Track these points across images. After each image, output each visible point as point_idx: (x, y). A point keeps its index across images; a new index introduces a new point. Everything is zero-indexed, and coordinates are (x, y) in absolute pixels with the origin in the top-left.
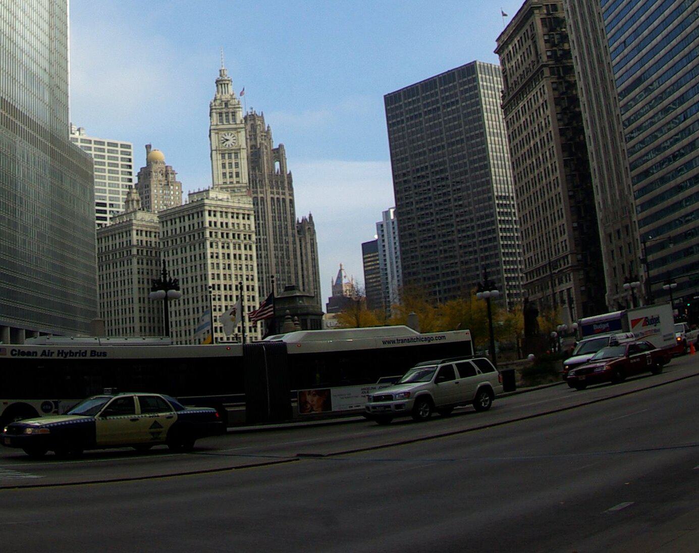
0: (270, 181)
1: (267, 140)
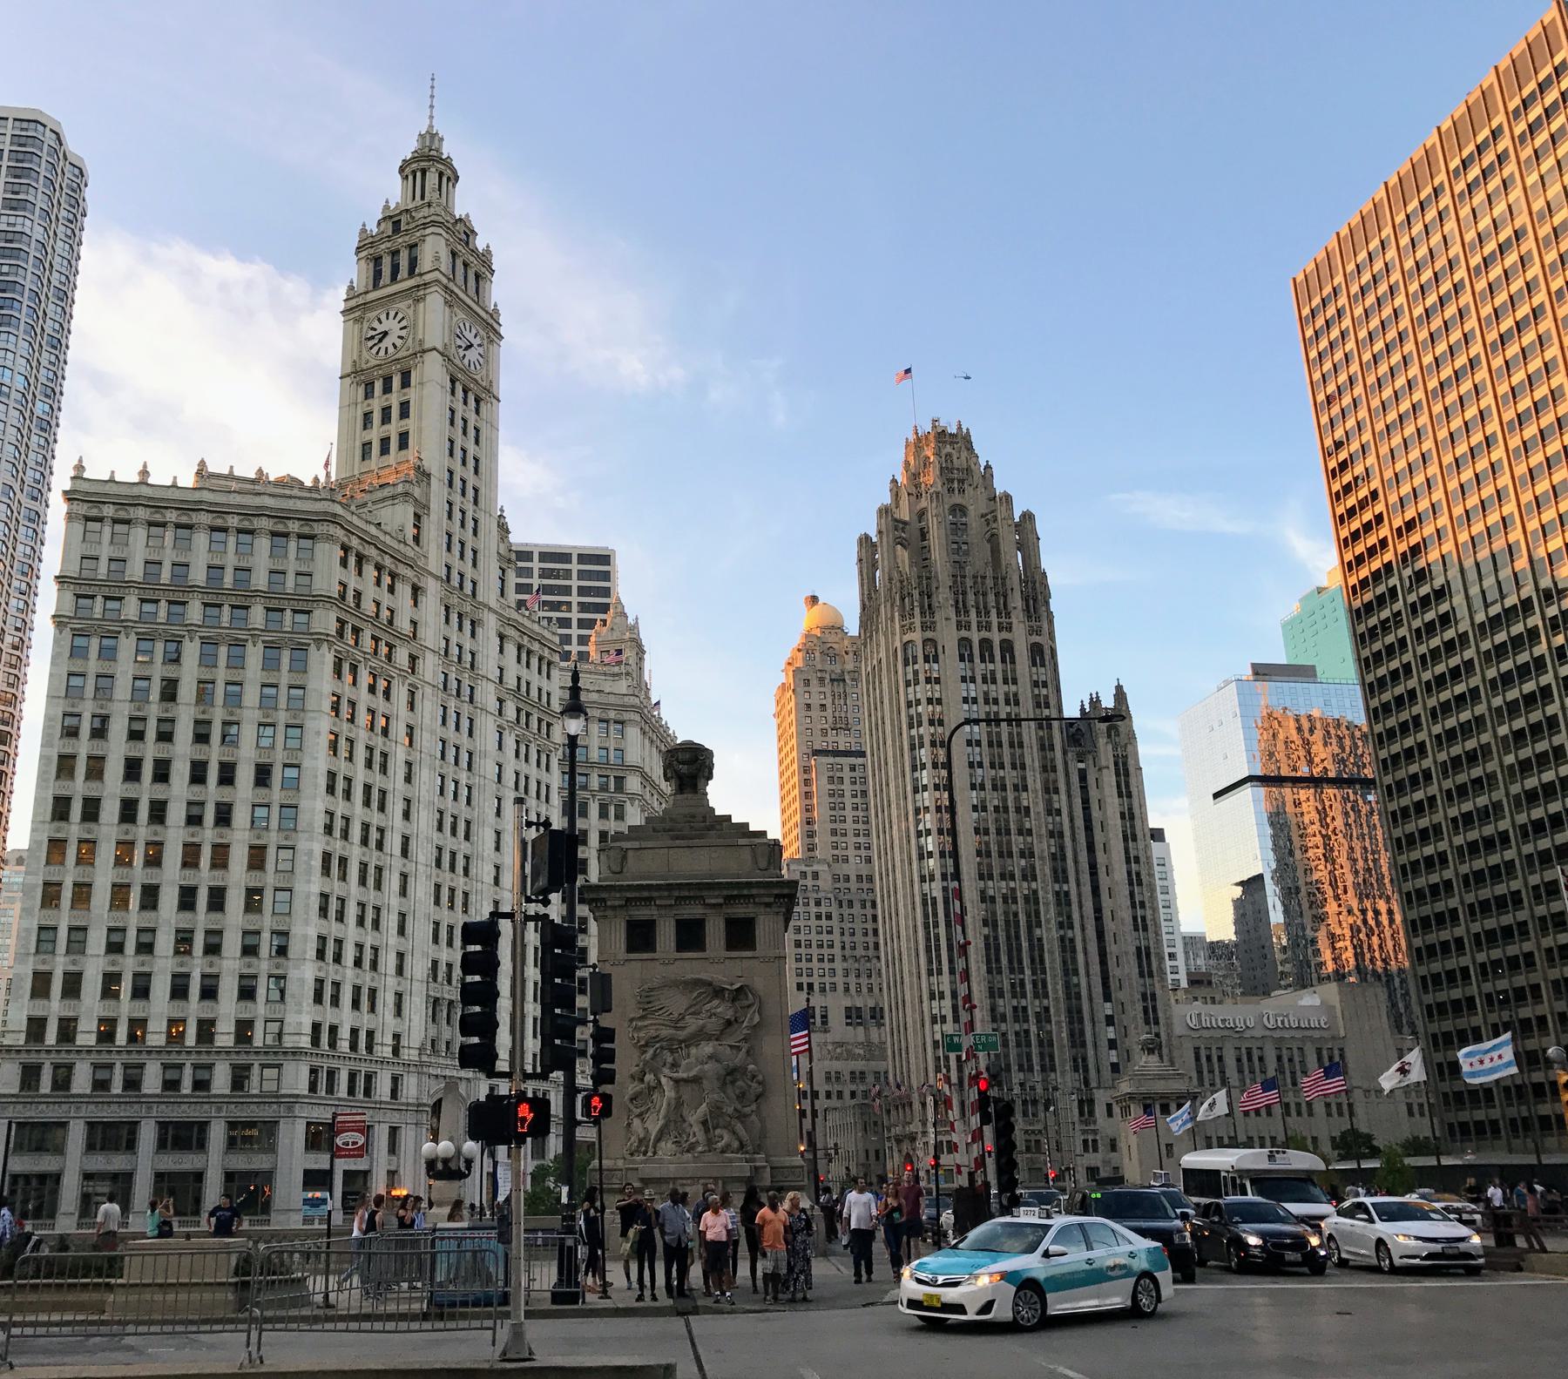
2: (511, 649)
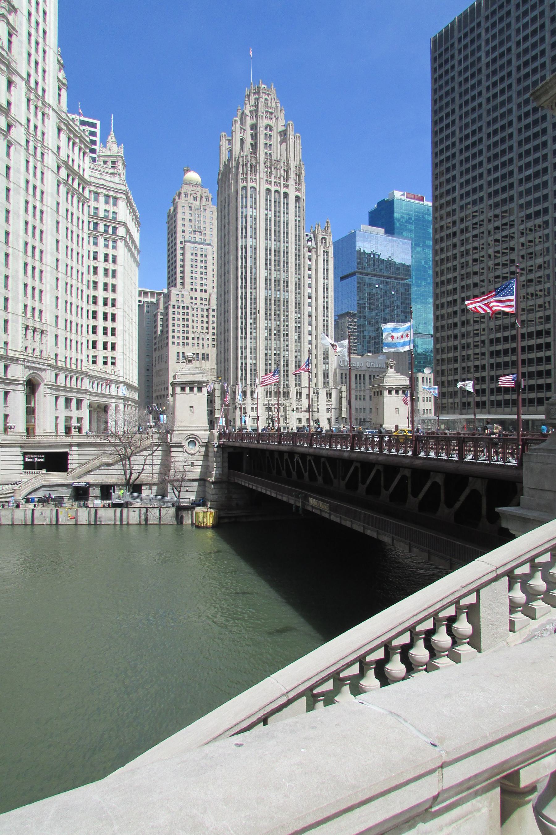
1: (274, 120)
2: (63, 137)
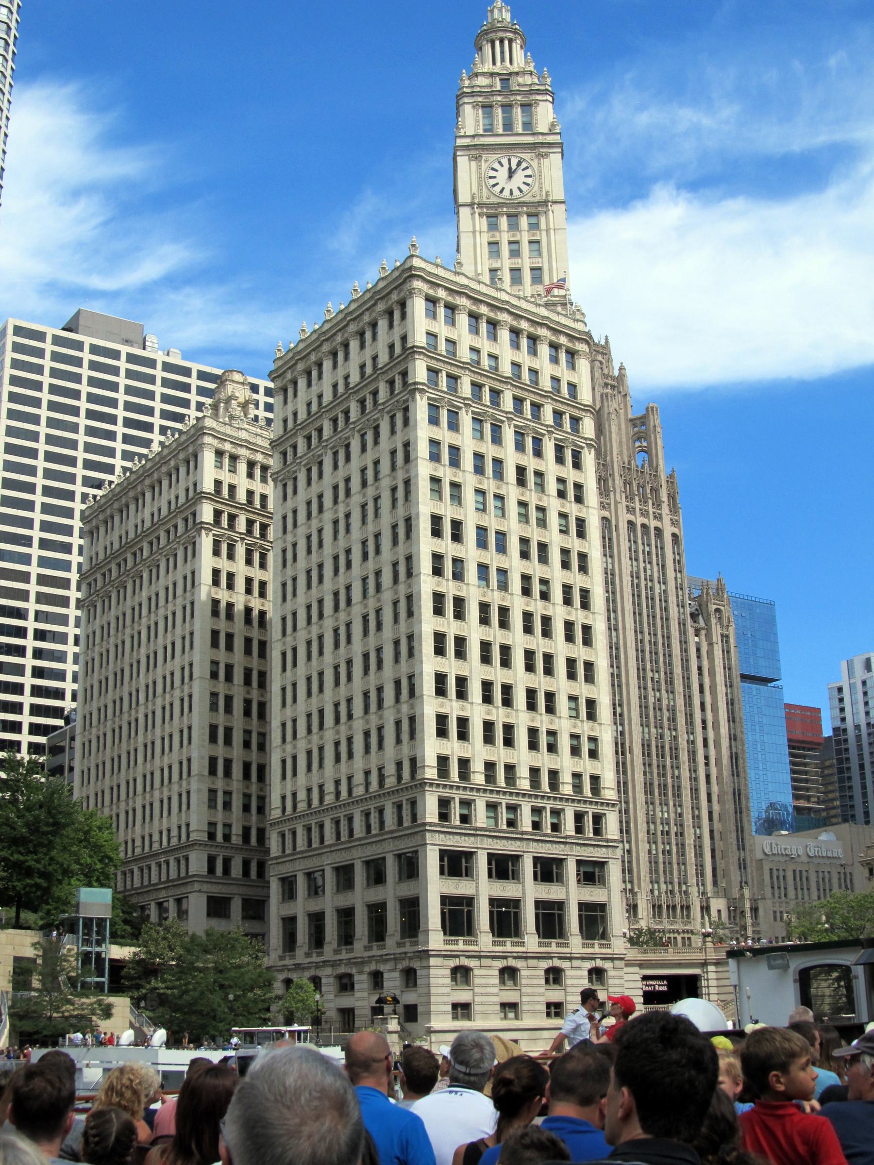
0: (627, 483)
